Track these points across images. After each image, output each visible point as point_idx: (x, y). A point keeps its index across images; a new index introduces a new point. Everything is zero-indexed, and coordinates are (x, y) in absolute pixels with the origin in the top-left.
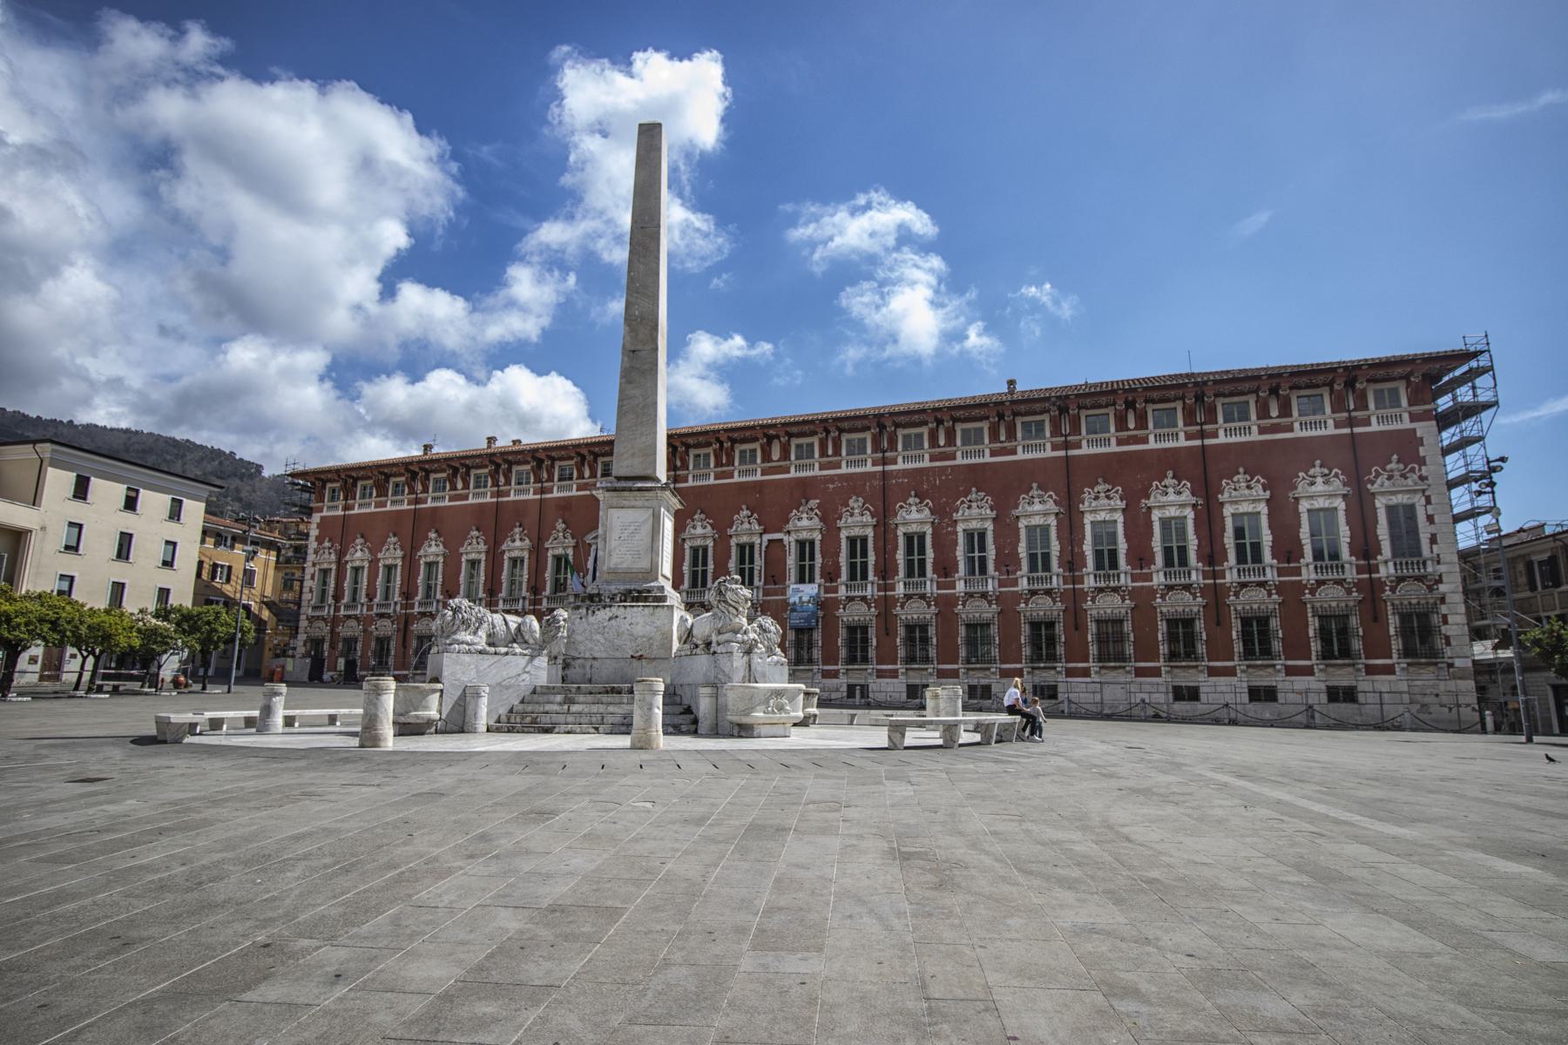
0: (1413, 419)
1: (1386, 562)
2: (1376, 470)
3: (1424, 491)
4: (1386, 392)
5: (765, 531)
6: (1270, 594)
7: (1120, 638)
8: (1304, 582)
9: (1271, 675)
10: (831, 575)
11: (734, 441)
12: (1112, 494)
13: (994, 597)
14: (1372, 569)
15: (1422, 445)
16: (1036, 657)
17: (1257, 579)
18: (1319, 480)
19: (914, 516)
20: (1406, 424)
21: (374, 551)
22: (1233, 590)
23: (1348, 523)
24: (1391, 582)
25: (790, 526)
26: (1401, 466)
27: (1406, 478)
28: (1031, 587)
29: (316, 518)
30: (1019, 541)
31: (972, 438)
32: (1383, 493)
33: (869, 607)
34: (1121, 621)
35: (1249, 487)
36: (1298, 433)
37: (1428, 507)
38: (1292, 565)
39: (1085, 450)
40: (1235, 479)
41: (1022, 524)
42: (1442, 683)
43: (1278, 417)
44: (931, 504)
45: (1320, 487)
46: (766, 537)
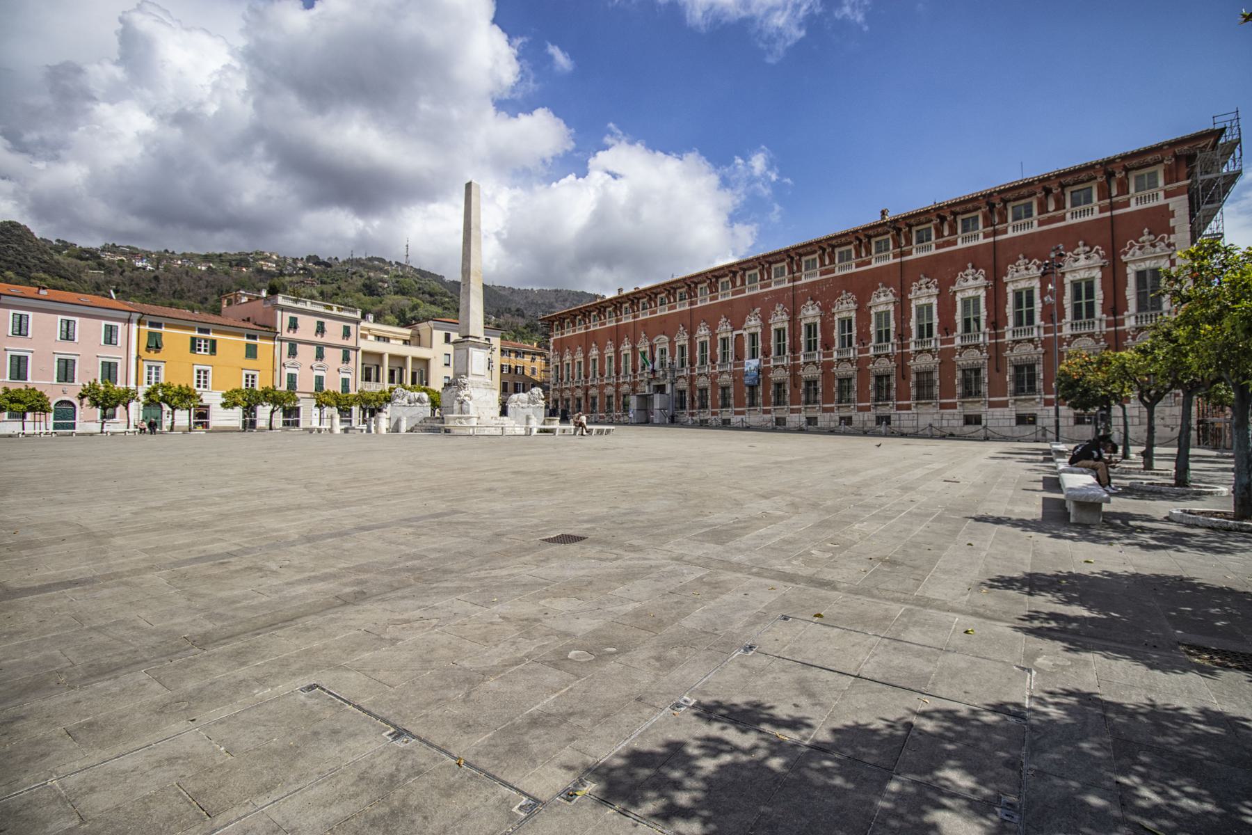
0: (1168, 195)
2: (1131, 244)
3: (1170, 255)
4: (1146, 176)
5: (734, 330)
6: (1036, 347)
7: (931, 384)
9: (1033, 405)
10: (766, 353)
11: (801, 255)
12: (930, 285)
15: (1173, 217)
16: (1018, 391)
17: (1027, 337)
19: (811, 312)
20: (1162, 201)
21: (573, 355)
23: (1103, 288)
25: (745, 326)
26: (1152, 237)
29: (551, 340)
30: (870, 322)
31: (845, 257)
32: (1134, 262)
34: (931, 372)
35: (1027, 269)
39: (915, 255)
42: (1167, 409)
43: (1055, 211)
45: (1082, 262)
46: (735, 333)
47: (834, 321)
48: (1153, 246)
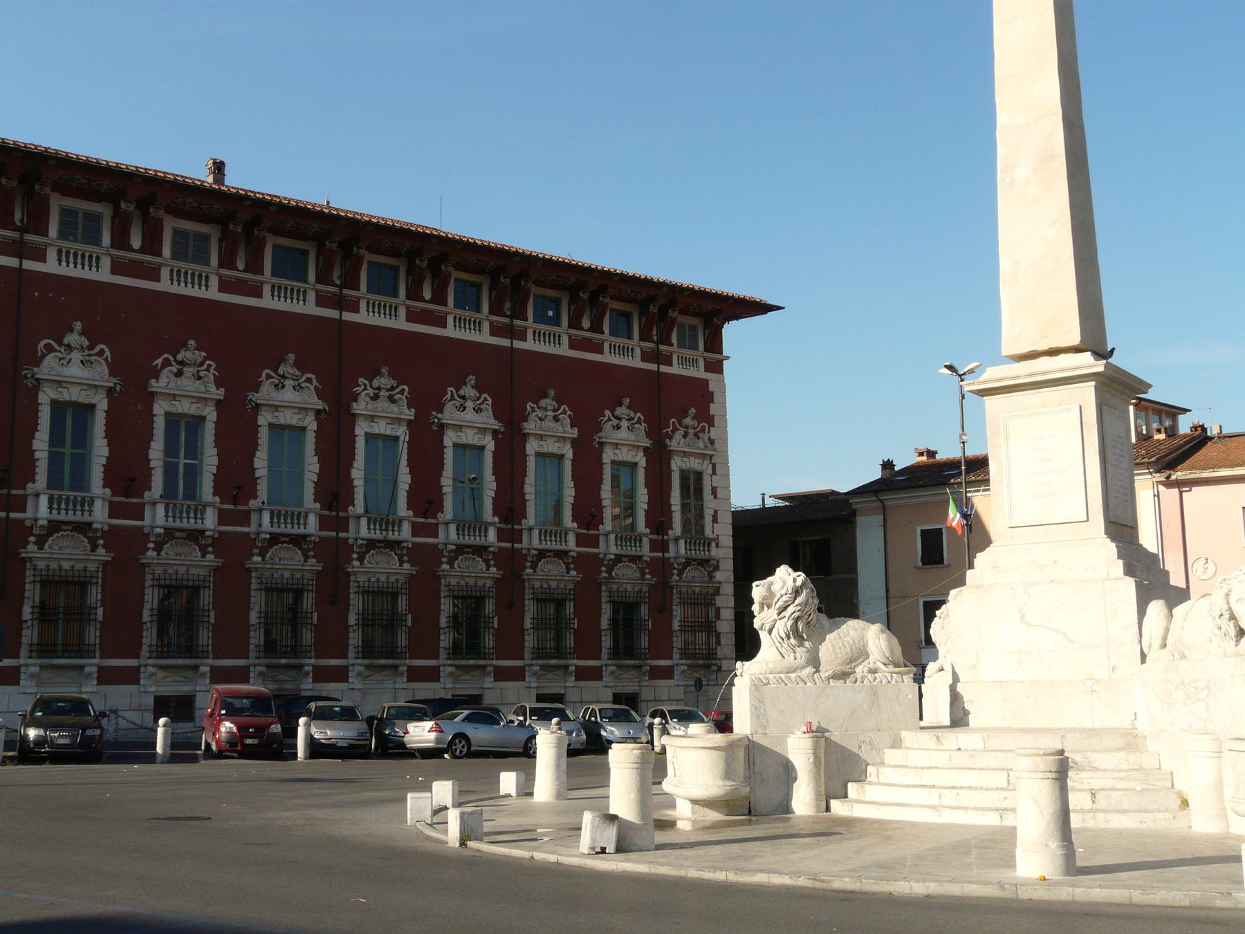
1: (676, 540)
6: (568, 570)
13: (210, 541)
18: (624, 424)
19: (75, 370)
22: (529, 559)
23: (646, 486)
27: (698, 438)
33: (94, 547)
35: (556, 419)
36: (608, 358)
37: (714, 476)
38: (591, 532)
39: (363, 317)
40: (543, 403)
41: (264, 419)
44: (108, 353)
45: (623, 435)
47: (151, 416)
48: (696, 435)
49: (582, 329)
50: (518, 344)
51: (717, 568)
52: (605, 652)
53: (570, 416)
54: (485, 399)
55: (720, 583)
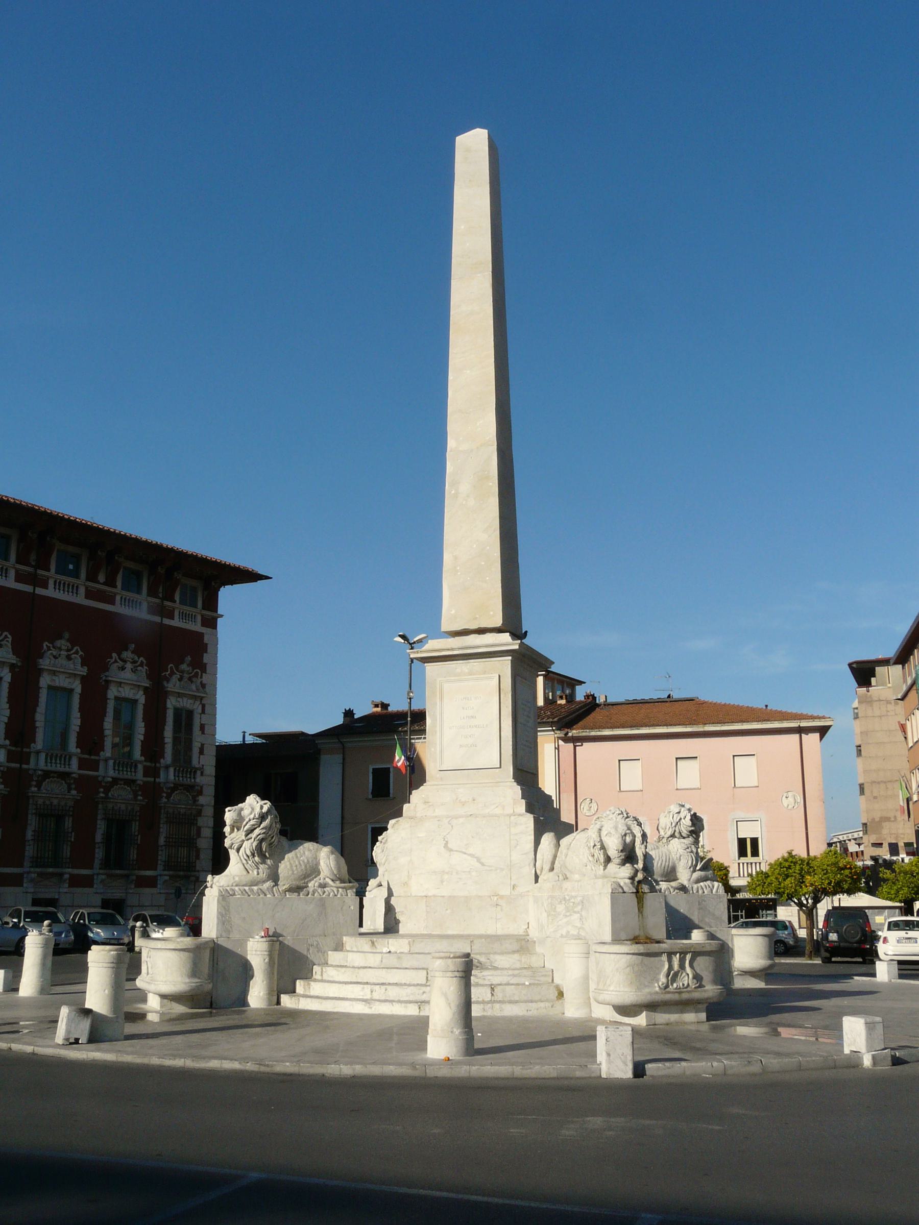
1: (167, 767)
6: (69, 790)
8: (100, 779)
14: (155, 772)
18: (129, 666)
22: (35, 778)
24: (168, 788)
27: (192, 682)
28: (49, 768)
35: (69, 658)
37: (202, 715)
38: (93, 757)
40: (58, 643)
45: (127, 675)
48: (190, 679)
49: (98, 582)
50: (40, 591)
51: (200, 793)
52: (97, 863)
53: (81, 656)
54: (6, 637)
55: (202, 806)
